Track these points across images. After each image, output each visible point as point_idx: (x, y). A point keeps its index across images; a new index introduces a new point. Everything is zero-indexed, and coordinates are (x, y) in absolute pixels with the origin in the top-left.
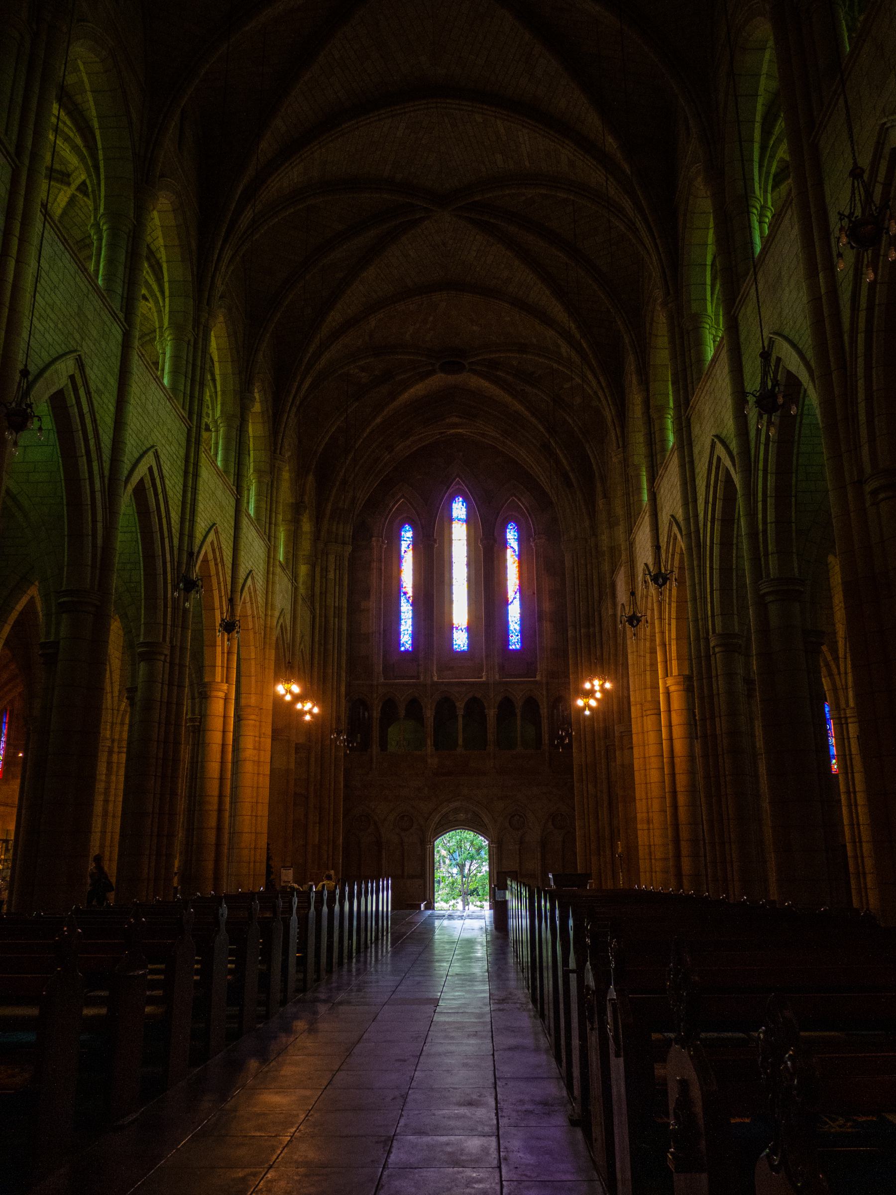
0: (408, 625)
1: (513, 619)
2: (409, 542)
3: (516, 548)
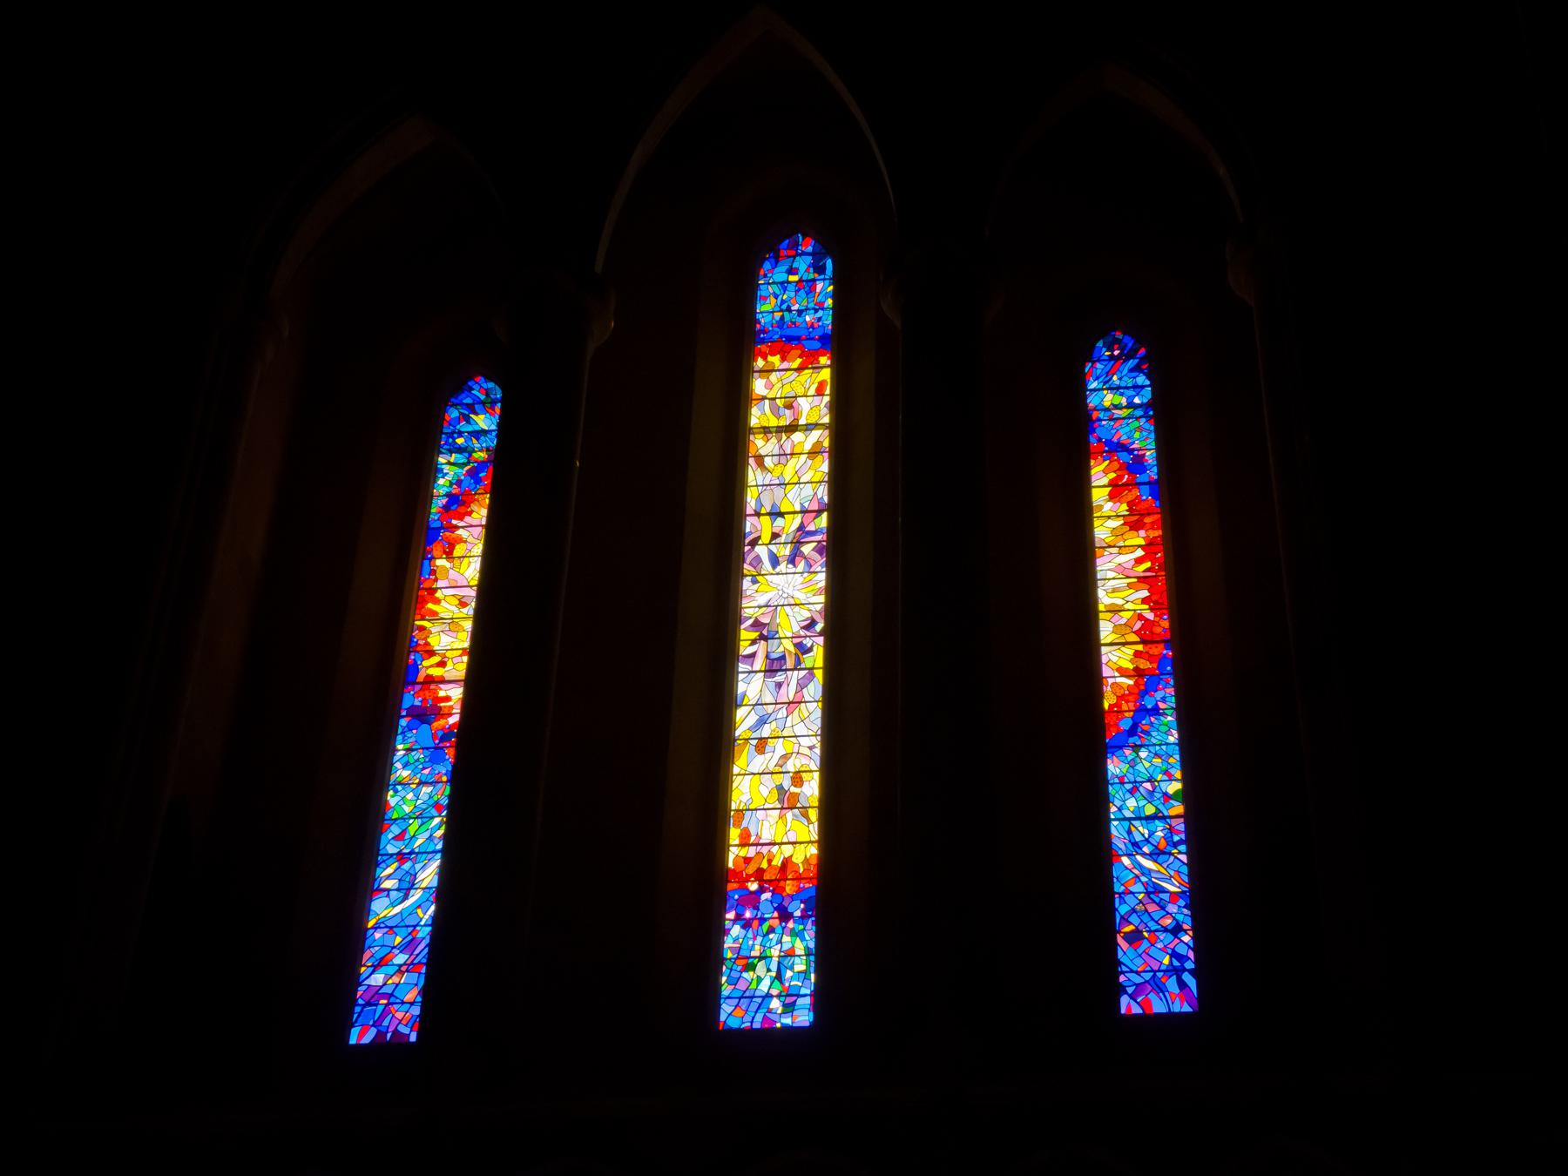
1: (1141, 830)
2: (480, 456)
3: (1143, 439)
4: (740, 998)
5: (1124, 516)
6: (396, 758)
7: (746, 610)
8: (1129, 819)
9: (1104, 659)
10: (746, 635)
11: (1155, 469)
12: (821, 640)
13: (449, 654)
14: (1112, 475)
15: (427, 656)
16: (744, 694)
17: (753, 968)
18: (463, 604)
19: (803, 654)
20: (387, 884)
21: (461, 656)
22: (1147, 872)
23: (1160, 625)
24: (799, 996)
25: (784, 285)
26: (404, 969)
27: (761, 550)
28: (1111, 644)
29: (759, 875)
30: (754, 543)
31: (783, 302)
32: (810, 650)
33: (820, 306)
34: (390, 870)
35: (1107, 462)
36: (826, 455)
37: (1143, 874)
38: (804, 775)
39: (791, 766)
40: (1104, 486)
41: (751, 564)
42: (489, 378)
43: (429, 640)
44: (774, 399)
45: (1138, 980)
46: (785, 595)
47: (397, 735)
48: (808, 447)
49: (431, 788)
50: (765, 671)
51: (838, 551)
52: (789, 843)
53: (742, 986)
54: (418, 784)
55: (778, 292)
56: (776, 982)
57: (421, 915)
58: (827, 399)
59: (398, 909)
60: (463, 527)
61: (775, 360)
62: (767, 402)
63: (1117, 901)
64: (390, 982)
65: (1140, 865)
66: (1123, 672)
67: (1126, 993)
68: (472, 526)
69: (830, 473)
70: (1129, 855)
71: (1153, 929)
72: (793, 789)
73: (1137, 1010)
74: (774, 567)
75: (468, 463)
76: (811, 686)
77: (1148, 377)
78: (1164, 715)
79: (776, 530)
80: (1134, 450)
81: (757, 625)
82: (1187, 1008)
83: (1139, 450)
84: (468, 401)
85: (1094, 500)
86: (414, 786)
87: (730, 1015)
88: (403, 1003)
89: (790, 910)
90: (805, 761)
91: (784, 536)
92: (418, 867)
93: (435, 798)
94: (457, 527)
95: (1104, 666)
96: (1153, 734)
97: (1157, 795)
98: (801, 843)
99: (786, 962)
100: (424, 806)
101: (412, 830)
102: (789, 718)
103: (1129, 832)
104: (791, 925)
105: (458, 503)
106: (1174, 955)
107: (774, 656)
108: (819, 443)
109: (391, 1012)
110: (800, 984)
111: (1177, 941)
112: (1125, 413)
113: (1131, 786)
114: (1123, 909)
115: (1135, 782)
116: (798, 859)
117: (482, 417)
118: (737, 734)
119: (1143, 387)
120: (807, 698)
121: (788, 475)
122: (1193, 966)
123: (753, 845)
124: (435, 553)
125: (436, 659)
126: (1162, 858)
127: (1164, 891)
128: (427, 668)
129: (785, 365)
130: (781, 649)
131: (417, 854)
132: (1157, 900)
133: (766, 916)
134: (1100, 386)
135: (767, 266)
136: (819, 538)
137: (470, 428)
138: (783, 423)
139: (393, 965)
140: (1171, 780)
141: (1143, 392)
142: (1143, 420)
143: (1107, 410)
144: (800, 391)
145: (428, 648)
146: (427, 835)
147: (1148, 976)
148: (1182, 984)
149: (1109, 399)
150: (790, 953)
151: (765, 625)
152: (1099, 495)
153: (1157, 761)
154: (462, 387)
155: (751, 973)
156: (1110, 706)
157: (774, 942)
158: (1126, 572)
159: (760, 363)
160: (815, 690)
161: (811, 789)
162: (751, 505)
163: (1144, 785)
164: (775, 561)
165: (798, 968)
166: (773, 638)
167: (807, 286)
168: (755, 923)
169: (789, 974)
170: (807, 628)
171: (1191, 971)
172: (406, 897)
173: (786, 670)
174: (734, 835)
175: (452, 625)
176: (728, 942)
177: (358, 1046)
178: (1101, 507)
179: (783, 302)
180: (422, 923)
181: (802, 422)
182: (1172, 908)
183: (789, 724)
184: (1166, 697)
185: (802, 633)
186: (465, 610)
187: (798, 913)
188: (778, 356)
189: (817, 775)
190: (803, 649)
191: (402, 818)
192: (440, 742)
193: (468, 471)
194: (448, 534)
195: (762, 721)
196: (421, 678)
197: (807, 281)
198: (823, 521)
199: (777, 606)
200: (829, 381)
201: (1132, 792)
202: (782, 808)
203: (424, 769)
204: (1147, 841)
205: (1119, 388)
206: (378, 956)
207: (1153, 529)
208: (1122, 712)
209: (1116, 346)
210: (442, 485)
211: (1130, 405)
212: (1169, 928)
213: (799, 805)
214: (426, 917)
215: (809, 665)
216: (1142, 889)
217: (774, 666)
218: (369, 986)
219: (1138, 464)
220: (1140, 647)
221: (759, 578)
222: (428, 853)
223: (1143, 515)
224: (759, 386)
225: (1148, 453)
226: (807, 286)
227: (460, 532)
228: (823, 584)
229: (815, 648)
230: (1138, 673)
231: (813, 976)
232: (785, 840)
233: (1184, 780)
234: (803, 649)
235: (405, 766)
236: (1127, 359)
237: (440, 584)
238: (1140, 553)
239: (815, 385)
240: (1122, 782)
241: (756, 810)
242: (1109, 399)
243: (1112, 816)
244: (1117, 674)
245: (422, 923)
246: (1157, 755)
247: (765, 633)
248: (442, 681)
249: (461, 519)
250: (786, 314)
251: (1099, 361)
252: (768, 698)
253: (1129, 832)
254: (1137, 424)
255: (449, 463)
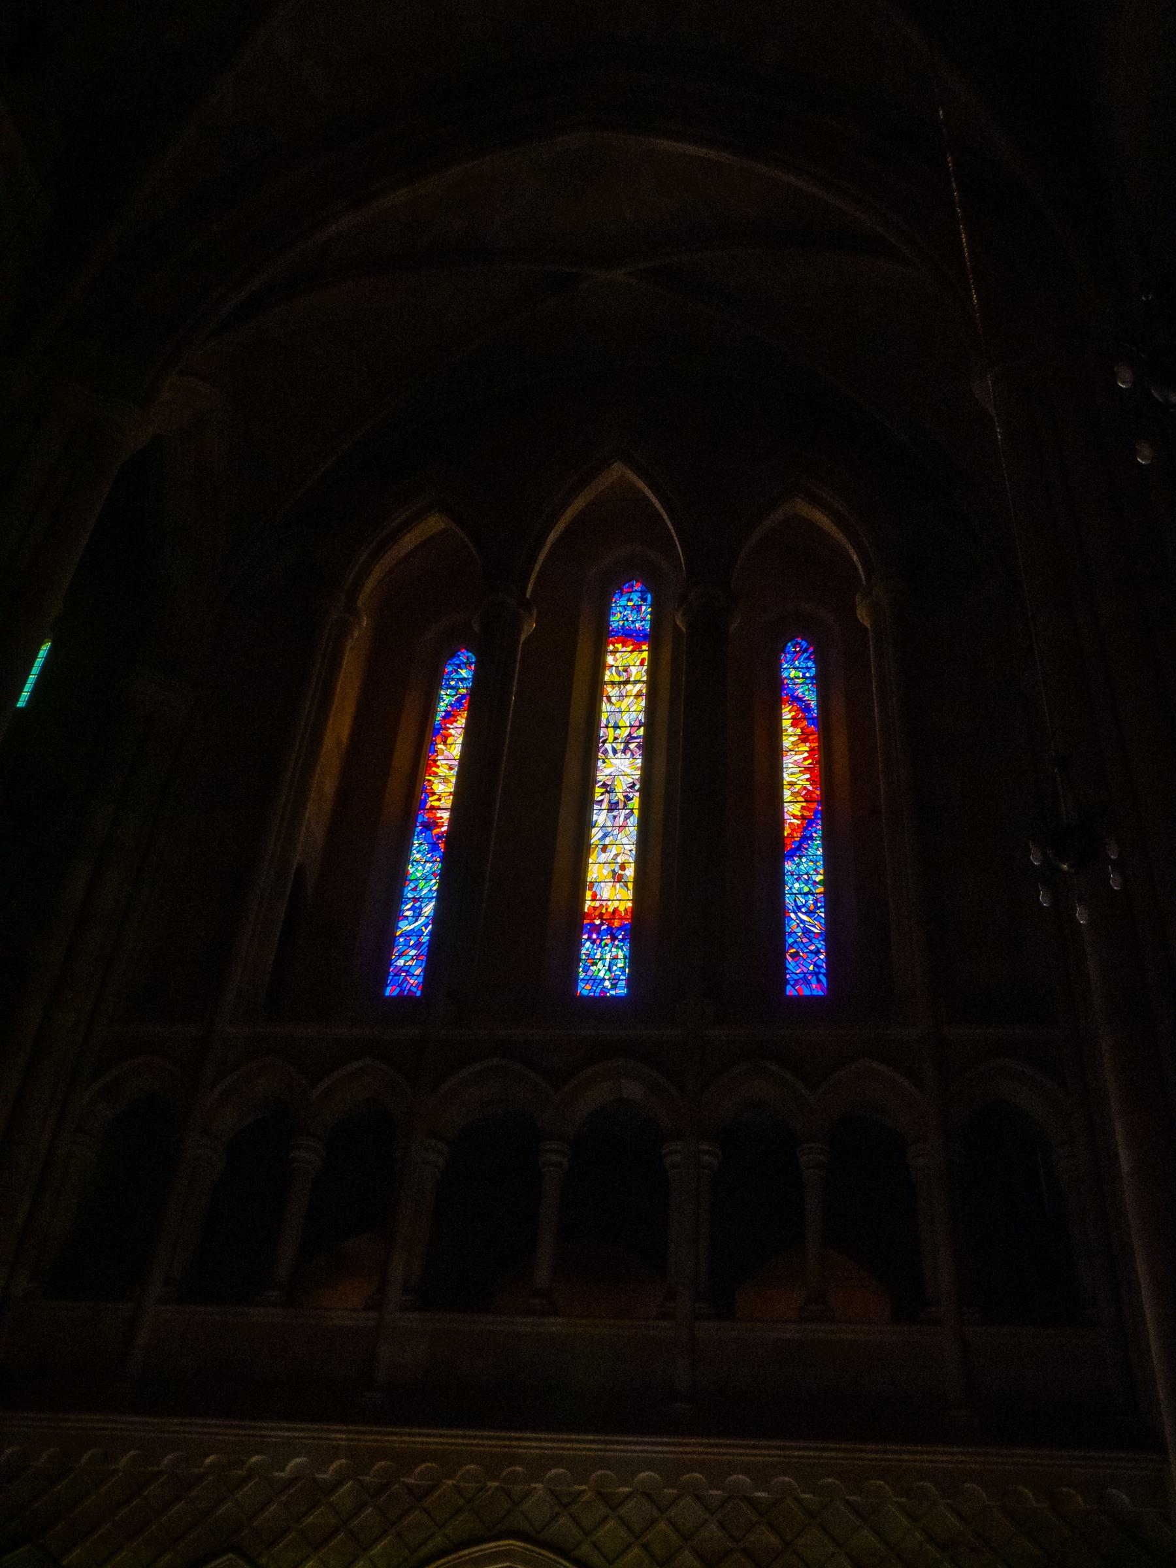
0: (422, 920)
1: (801, 900)
2: (463, 691)
3: (811, 698)
4: (588, 980)
5: (799, 735)
6: (414, 848)
7: (599, 777)
8: (795, 894)
9: (786, 810)
10: (598, 790)
11: (816, 711)
12: (637, 794)
13: (442, 794)
14: (793, 713)
15: (430, 795)
16: (596, 821)
17: (596, 964)
18: (451, 768)
19: (628, 801)
20: (407, 913)
21: (449, 796)
22: (802, 921)
23: (815, 793)
24: (619, 980)
25: (625, 607)
26: (414, 957)
27: (608, 746)
28: (789, 802)
29: (603, 914)
30: (604, 742)
31: (624, 616)
32: (632, 799)
33: (644, 619)
34: (408, 906)
35: (791, 706)
36: (644, 697)
37: (801, 923)
38: (626, 865)
39: (620, 860)
40: (789, 719)
41: (602, 753)
42: (468, 651)
43: (433, 787)
44: (617, 667)
45: (796, 977)
46: (620, 770)
47: (414, 836)
48: (634, 692)
49: (431, 864)
50: (608, 809)
51: (648, 749)
52: (617, 900)
53: (590, 973)
54: (425, 862)
55: (621, 610)
56: (608, 972)
57: (424, 930)
58: (645, 668)
59: (412, 927)
60: (452, 728)
61: (619, 646)
62: (614, 668)
63: (787, 936)
64: (407, 964)
65: (800, 917)
66: (795, 817)
67: (789, 984)
68: (457, 728)
69: (645, 707)
70: (795, 913)
71: (805, 951)
72: (620, 872)
73: (795, 993)
74: (614, 755)
75: (455, 695)
76: (632, 818)
77: (814, 662)
78: (816, 840)
79: (616, 736)
80: (805, 700)
81: (604, 785)
82: (821, 993)
83: (808, 700)
84: (457, 662)
85: (783, 725)
86: (422, 863)
87: (584, 989)
88: (413, 975)
89: (616, 935)
90: (627, 857)
91: (620, 739)
92: (423, 905)
93: (433, 870)
94: (450, 728)
95: (785, 814)
96: (810, 850)
97: (811, 882)
98: (623, 900)
99: (614, 962)
100: (427, 874)
101: (420, 886)
102: (620, 835)
103: (795, 901)
104: (616, 943)
105: (450, 716)
106: (815, 965)
107: (613, 801)
108: (640, 691)
109: (407, 980)
110: (620, 974)
111: (817, 958)
112: (800, 681)
113: (797, 876)
114: (790, 941)
115: (799, 875)
116: (622, 909)
117: (465, 671)
118: (592, 842)
119: (811, 668)
120: (629, 824)
121: (624, 706)
122: (825, 971)
123: (598, 900)
124: (437, 742)
125: (436, 797)
126: (811, 915)
127: (813, 932)
128: (431, 801)
129: (624, 649)
130: (616, 798)
131: (423, 898)
132: (808, 936)
133: (604, 938)
134: (789, 666)
135: (617, 596)
136: (639, 740)
137: (457, 677)
138: (622, 679)
139: (409, 955)
140: (817, 874)
141: (811, 671)
142: (811, 685)
143: (792, 679)
144: (632, 663)
145: (432, 791)
146: (429, 888)
147: (802, 976)
148: (819, 981)
149: (793, 673)
150: (616, 958)
151: (609, 785)
152: (786, 723)
153: (811, 864)
154: (454, 655)
155: (595, 967)
156: (788, 834)
157: (607, 951)
158: (801, 765)
159: (611, 647)
160: (633, 820)
161: (630, 872)
162: (604, 722)
163: (804, 876)
164: (615, 751)
165: (619, 965)
166: (612, 792)
167: (637, 608)
168: (598, 941)
169: (615, 968)
170: (630, 787)
171: (824, 974)
172: (416, 921)
173: (619, 809)
174: (589, 894)
175: (445, 780)
176: (584, 951)
177: (390, 997)
178: (787, 730)
179: (624, 616)
180: (425, 934)
181: (632, 679)
182: (815, 941)
183: (619, 838)
184: (817, 832)
185: (628, 790)
186: (452, 772)
187: (620, 937)
188: (621, 645)
189: (633, 865)
190: (628, 798)
191: (416, 880)
192: (437, 840)
193: (456, 699)
194: (444, 731)
195: (605, 836)
196: (427, 807)
197: (637, 606)
198: (641, 732)
199: (615, 776)
200: (647, 658)
201: (797, 880)
202: (614, 882)
203: (428, 854)
204: (804, 906)
205: (798, 668)
206: (401, 951)
207: (814, 742)
208: (794, 837)
209: (798, 646)
210: (443, 706)
211: (804, 677)
212: (814, 951)
213: (623, 880)
214: (427, 931)
215: (631, 807)
216: (800, 930)
217: (613, 807)
218: (396, 966)
219: (807, 708)
220: (804, 804)
221: (606, 760)
222: (429, 898)
223: (809, 735)
224: (610, 660)
225: (813, 702)
226: (637, 608)
227: (451, 731)
228: (640, 765)
229: (634, 798)
230: (803, 817)
231: (627, 970)
232: (615, 898)
233: (825, 874)
234: (628, 798)
235: (419, 852)
236: (802, 654)
237: (439, 758)
238: (806, 755)
239: (640, 660)
240: (792, 875)
241: (600, 882)
242: (793, 673)
243: (786, 892)
244: (792, 818)
245: (425, 934)
246: (811, 861)
247: (608, 789)
248: (439, 808)
249: (452, 724)
250: (626, 622)
251: (789, 653)
252: (609, 824)
253: (795, 901)
254: (807, 687)
255: (446, 694)
